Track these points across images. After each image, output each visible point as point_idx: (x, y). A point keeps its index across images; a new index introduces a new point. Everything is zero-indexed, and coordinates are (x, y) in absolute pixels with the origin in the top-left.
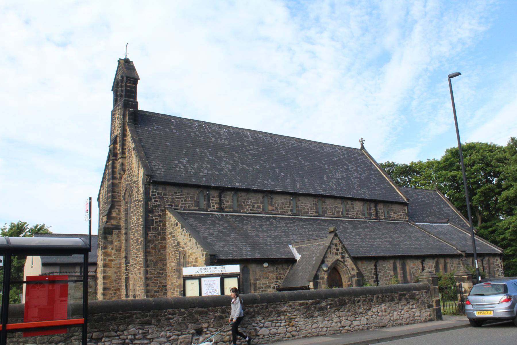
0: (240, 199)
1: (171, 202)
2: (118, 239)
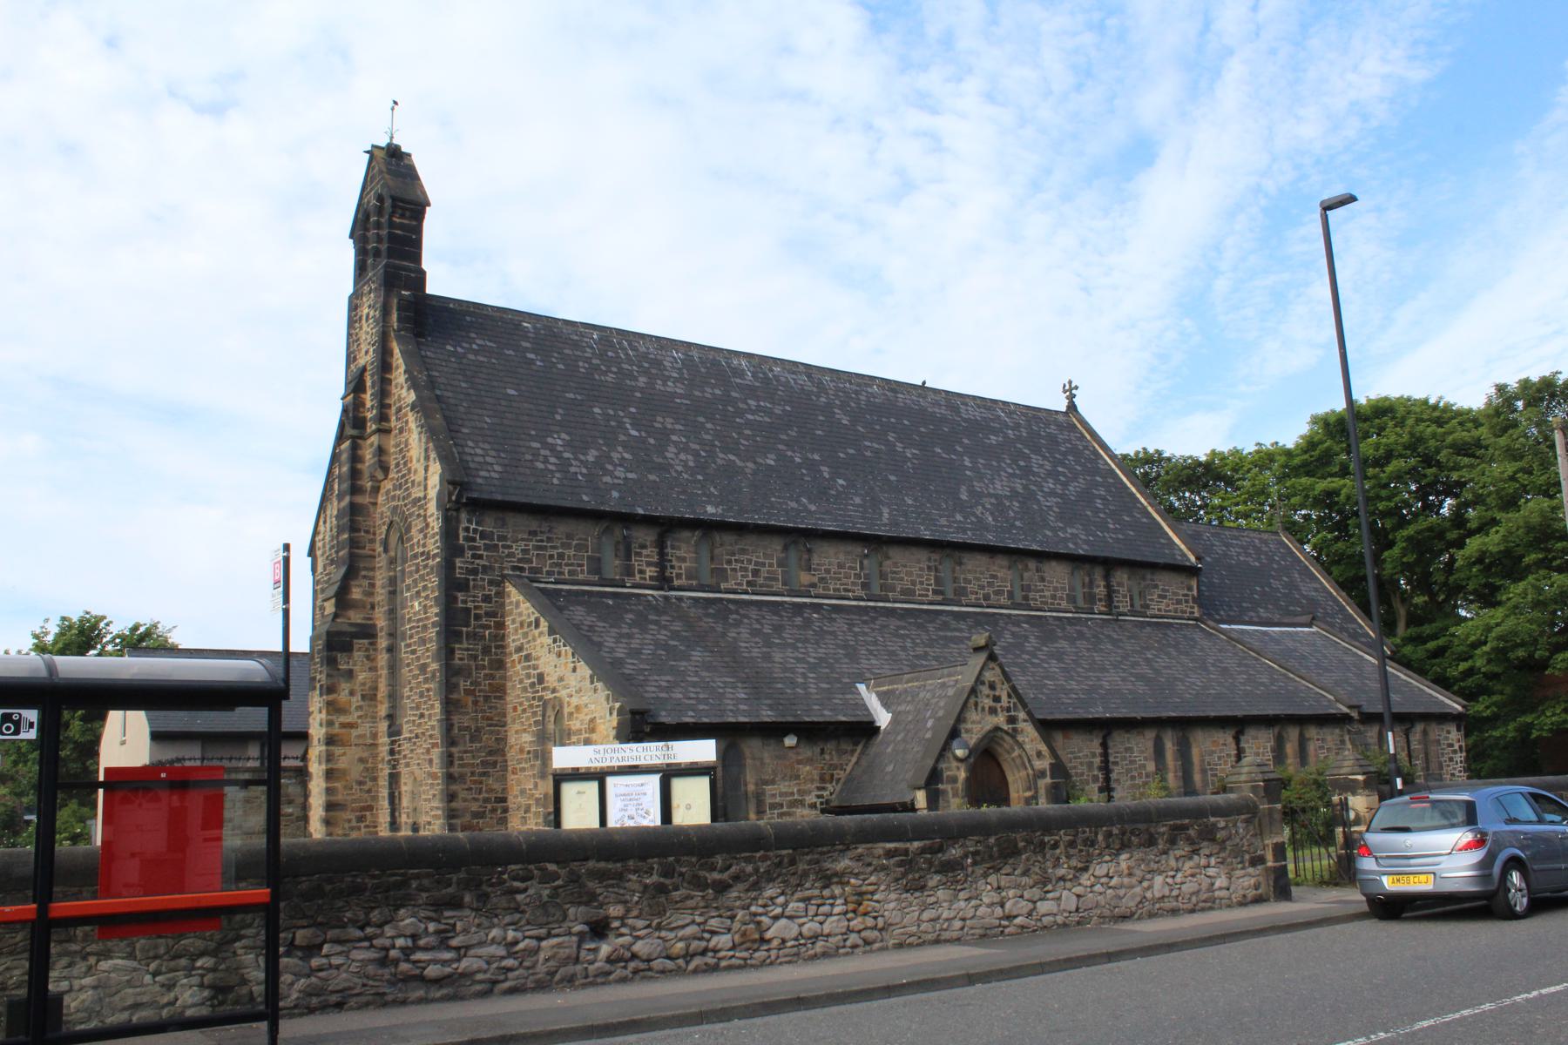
0: (717, 551)
1: (520, 560)
2: (368, 664)
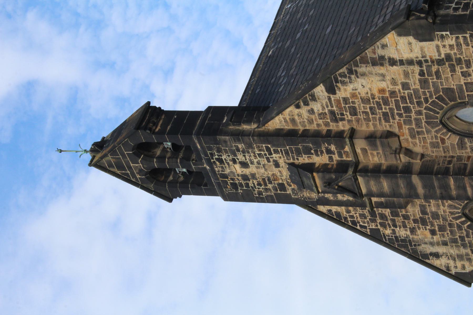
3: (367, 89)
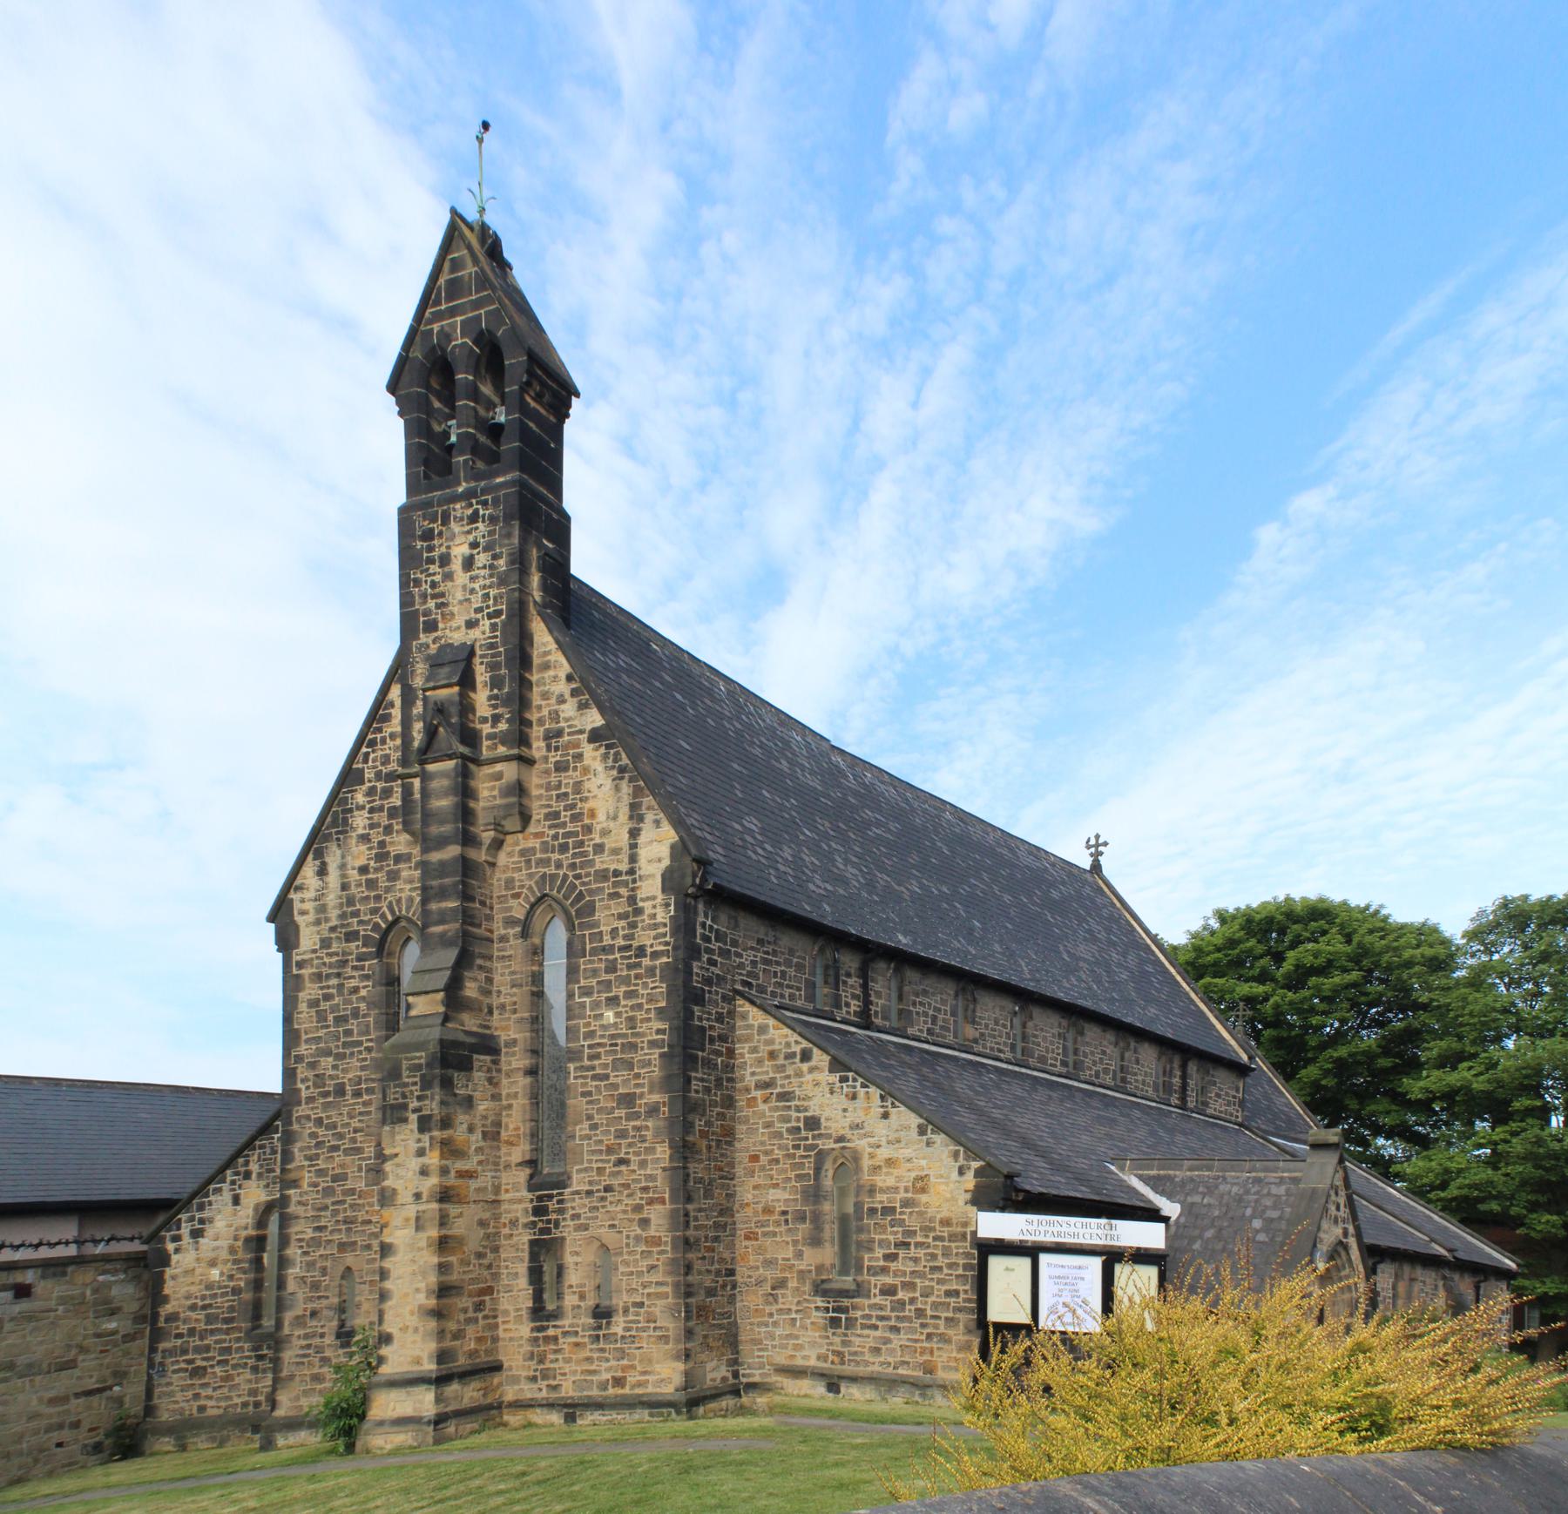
2: (491, 1090)
3: (595, 791)
